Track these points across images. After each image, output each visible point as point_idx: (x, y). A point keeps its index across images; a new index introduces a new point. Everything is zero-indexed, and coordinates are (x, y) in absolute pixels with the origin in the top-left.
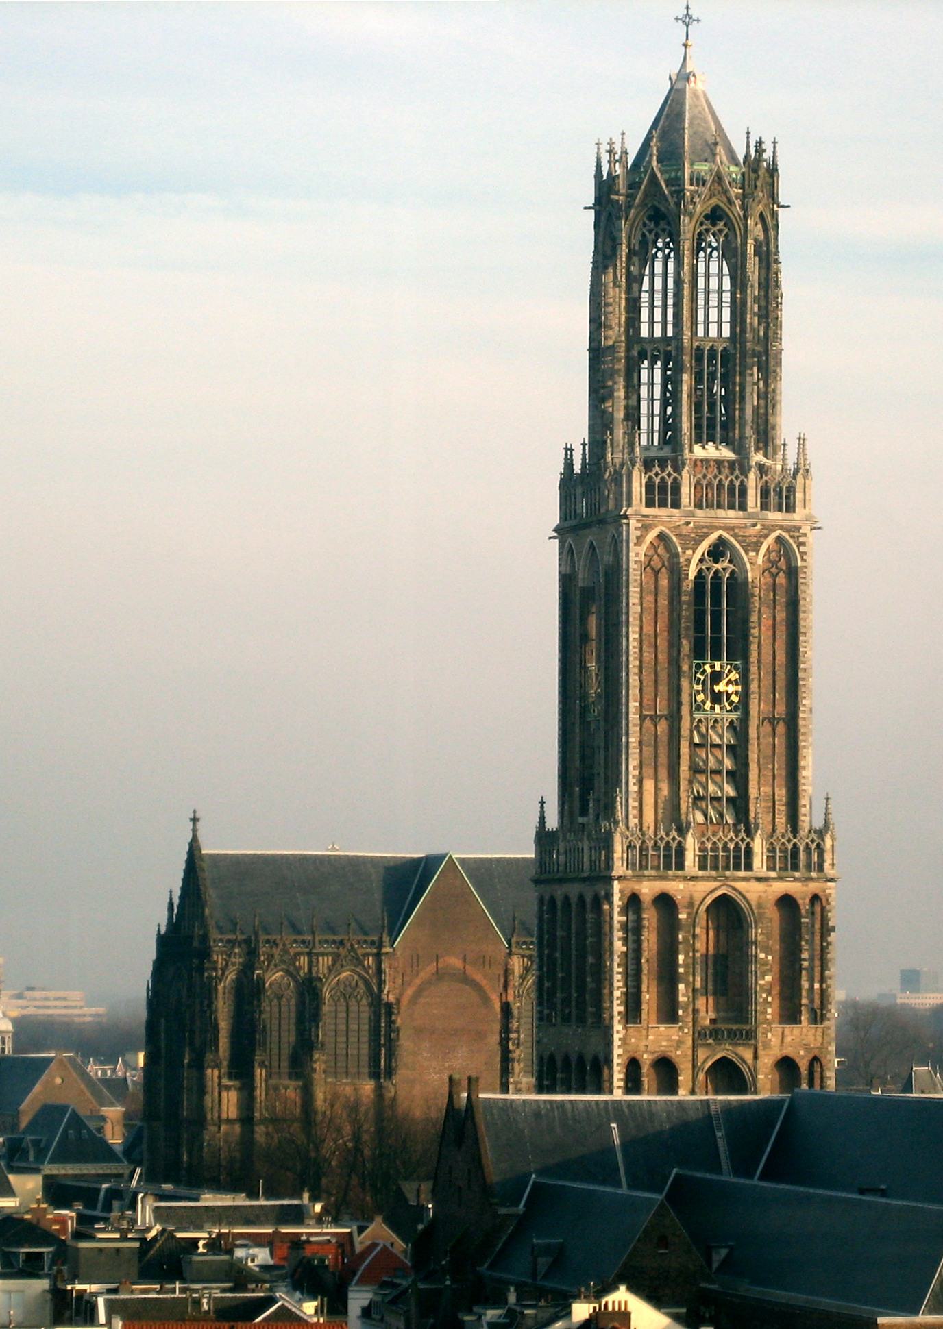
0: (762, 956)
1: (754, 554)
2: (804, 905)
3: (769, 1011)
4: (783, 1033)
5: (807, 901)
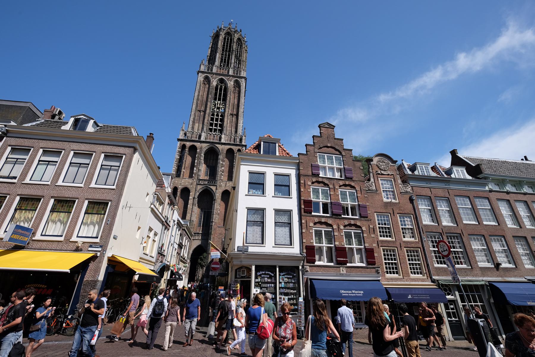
0: (222, 162)
2: (236, 151)
3: (222, 177)
4: (226, 183)
5: (237, 150)
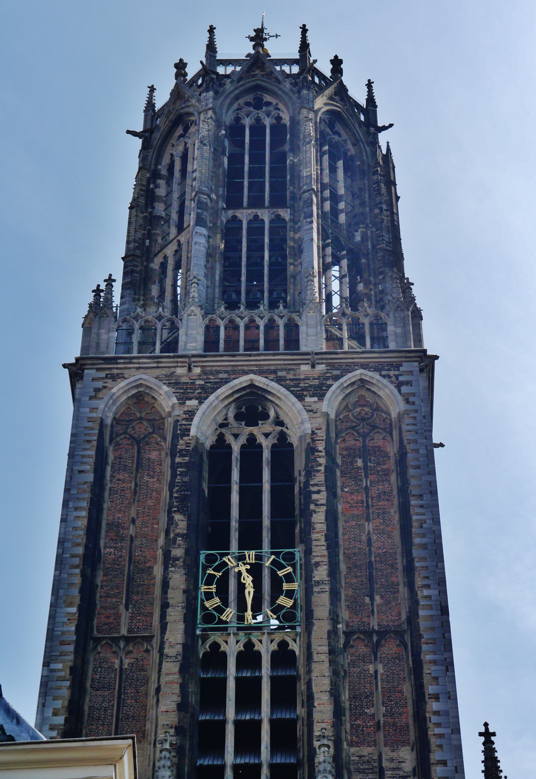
1: (316, 399)
